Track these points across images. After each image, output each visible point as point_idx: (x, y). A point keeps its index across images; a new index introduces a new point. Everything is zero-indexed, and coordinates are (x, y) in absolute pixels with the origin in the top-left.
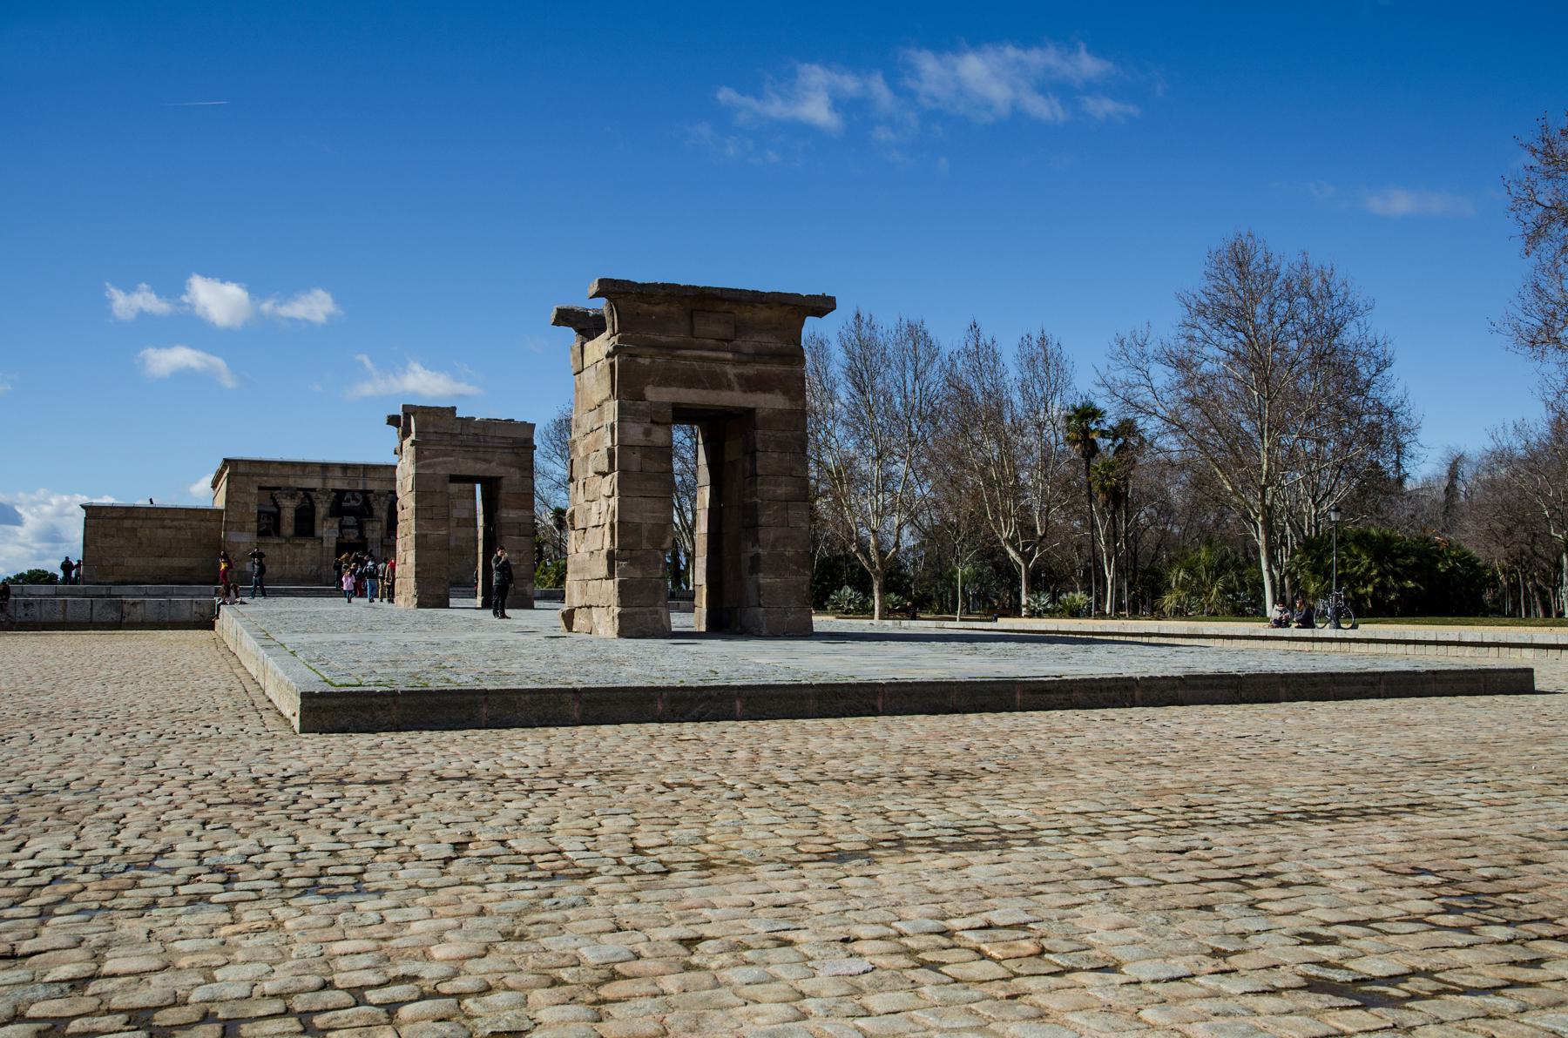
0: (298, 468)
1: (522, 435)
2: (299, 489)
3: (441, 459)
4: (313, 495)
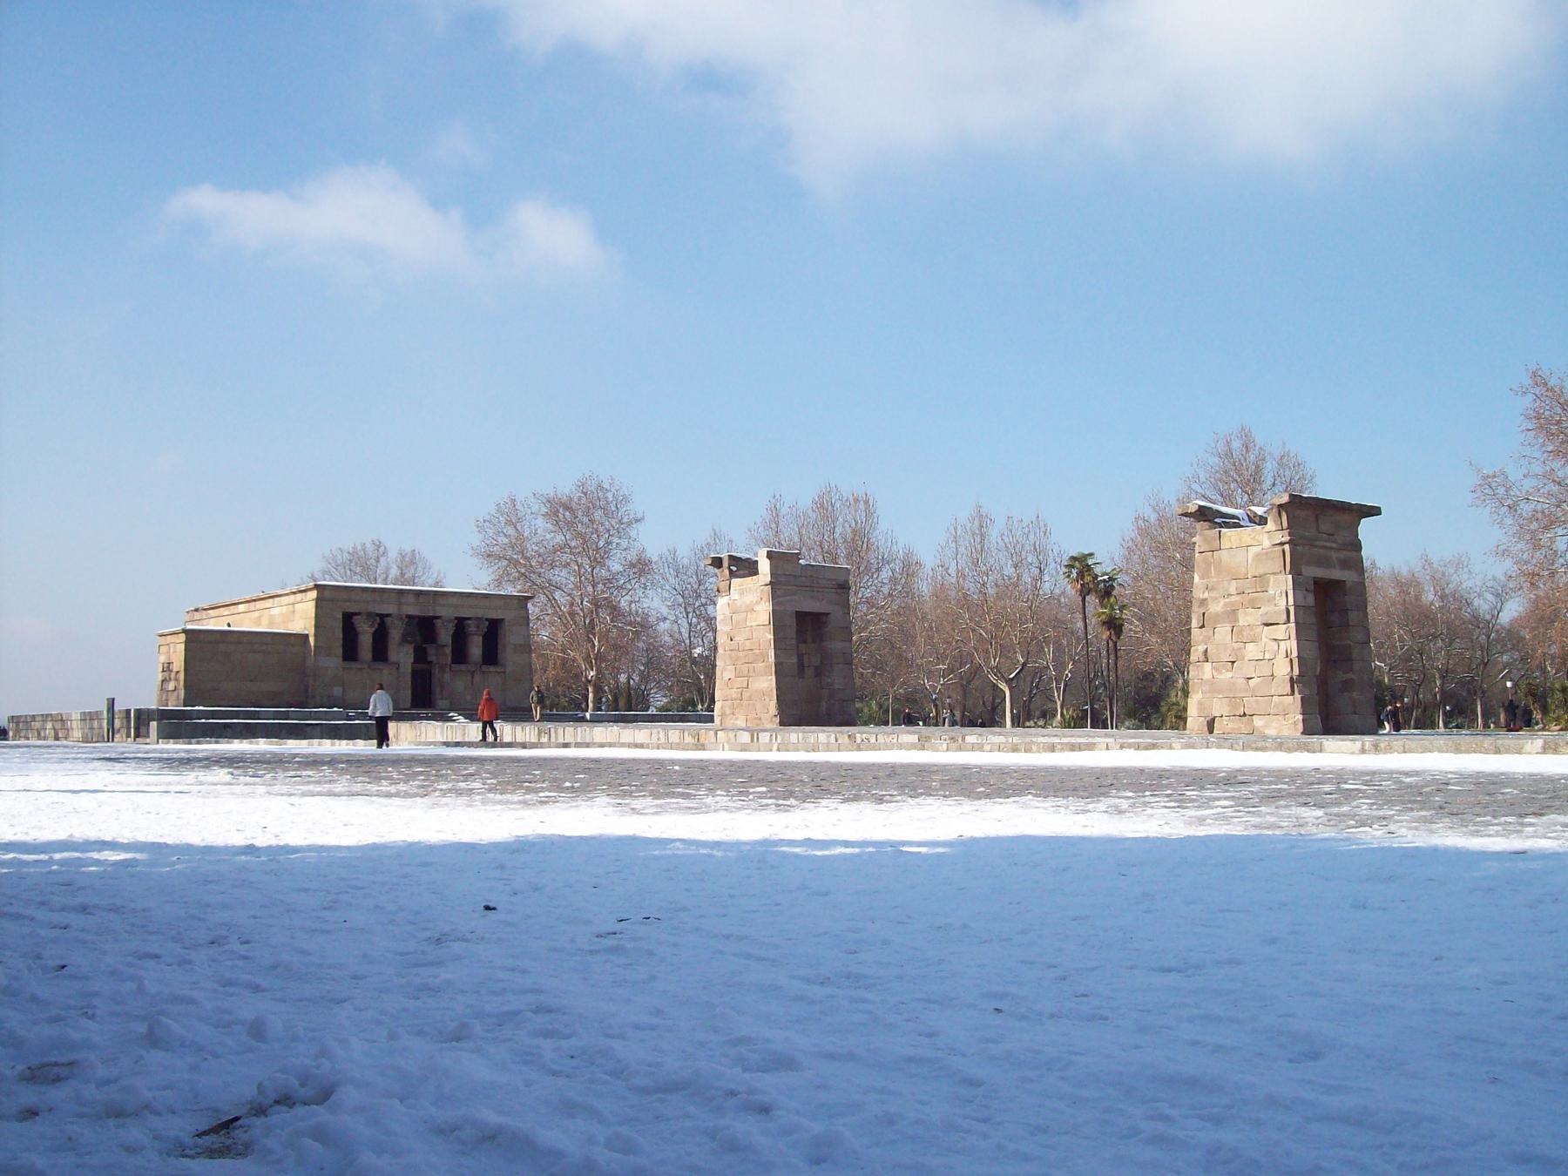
0: (377, 594)
1: (842, 578)
2: (378, 615)
3: (788, 598)
4: (388, 620)
